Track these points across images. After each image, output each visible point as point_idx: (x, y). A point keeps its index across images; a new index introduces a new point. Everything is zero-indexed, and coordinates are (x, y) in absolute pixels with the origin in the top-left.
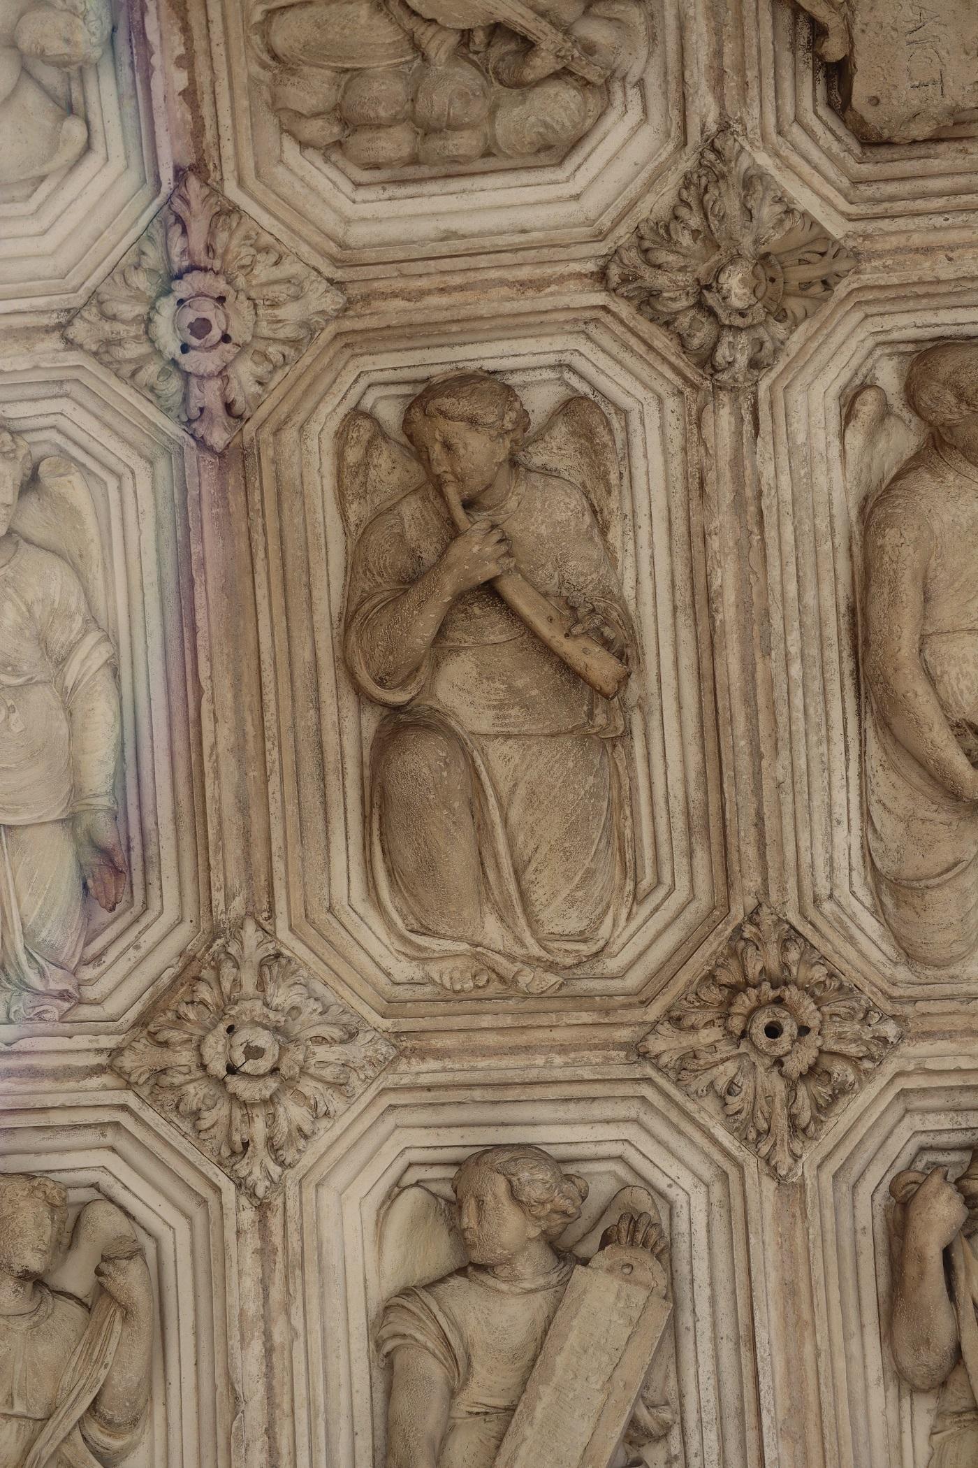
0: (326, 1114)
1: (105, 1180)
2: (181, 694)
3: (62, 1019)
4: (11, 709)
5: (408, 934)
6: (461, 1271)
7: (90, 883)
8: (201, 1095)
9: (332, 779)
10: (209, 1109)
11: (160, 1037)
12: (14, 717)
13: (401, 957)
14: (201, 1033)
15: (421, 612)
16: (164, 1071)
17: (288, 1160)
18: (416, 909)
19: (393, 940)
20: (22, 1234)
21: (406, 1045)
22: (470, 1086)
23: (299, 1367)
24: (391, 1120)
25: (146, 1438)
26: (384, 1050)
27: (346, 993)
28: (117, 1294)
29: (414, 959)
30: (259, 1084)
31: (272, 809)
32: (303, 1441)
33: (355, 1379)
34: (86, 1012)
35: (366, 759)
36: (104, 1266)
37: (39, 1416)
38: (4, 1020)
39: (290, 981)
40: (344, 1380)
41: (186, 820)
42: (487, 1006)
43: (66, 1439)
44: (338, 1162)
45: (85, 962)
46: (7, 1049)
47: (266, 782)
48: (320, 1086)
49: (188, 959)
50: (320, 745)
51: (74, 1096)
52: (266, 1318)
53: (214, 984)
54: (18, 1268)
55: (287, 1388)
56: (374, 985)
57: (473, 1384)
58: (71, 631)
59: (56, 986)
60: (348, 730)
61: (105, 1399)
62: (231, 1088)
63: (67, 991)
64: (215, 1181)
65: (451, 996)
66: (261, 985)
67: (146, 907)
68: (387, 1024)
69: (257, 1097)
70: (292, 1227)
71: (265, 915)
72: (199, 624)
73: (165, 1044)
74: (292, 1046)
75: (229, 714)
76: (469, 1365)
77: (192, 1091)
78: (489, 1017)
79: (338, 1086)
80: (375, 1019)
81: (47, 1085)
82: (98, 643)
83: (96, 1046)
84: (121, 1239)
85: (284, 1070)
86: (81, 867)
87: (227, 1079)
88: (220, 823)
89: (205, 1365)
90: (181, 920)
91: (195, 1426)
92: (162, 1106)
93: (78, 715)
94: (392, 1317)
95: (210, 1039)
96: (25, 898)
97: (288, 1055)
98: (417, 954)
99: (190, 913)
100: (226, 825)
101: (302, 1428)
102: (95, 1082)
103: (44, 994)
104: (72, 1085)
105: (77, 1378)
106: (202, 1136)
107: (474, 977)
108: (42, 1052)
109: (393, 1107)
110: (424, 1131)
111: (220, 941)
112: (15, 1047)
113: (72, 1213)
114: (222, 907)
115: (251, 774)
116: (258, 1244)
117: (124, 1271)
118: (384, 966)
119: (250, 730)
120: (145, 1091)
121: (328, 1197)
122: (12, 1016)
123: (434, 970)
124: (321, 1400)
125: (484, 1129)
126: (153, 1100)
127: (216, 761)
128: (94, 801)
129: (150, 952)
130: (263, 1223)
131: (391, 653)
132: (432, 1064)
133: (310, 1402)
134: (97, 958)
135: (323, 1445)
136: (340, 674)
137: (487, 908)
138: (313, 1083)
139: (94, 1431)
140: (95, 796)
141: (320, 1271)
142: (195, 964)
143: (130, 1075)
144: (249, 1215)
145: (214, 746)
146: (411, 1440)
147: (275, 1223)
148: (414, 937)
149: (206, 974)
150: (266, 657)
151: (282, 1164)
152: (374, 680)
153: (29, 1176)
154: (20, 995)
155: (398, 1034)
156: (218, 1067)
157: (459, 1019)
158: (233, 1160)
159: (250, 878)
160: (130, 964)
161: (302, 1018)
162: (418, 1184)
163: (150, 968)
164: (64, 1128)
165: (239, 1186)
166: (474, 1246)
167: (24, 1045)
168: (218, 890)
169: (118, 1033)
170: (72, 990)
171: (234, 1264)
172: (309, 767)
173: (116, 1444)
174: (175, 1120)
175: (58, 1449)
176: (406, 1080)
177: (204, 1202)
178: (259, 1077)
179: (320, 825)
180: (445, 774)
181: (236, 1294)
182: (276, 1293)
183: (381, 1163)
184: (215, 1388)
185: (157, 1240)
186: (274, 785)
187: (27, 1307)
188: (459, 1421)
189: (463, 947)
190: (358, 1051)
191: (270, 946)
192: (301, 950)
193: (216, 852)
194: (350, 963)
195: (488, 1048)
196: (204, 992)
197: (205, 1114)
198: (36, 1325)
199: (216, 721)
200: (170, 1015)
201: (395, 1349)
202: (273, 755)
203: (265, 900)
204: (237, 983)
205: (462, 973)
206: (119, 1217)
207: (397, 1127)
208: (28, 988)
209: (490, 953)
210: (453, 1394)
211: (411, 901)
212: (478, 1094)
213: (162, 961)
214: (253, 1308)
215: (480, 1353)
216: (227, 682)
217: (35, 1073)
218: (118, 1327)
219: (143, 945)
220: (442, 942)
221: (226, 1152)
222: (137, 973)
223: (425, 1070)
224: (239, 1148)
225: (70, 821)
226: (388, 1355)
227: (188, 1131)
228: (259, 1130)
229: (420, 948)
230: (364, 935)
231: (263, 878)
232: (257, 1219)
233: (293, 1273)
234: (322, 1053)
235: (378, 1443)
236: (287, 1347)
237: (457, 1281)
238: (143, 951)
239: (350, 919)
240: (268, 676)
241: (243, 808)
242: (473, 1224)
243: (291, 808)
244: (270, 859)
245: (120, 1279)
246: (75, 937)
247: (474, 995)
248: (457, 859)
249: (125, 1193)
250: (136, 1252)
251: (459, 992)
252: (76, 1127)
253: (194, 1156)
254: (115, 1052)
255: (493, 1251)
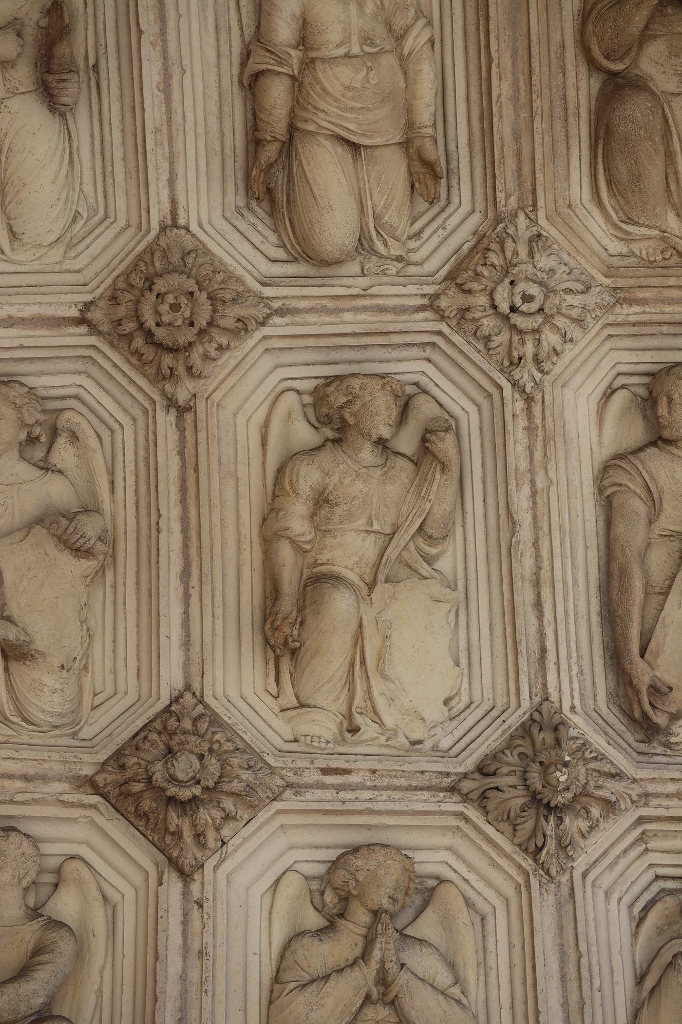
0: (571, 340)
1: (423, 381)
2: (476, 61)
3: (398, 274)
4: (370, 69)
5: (619, 223)
6: (653, 444)
7: (417, 185)
8: (491, 325)
9: (571, 119)
10: (497, 335)
11: (466, 287)
12: (372, 74)
13: (614, 239)
14: (492, 285)
15: (638, 11)
16: (468, 310)
17: (546, 369)
18: (625, 207)
19: (609, 227)
20: (377, 414)
21: (622, 296)
22: (660, 324)
23: (554, 504)
24: (608, 345)
25: (450, 548)
26: (607, 299)
27: (583, 261)
28: (436, 451)
29: (623, 240)
30: (530, 319)
31: (536, 139)
32: (557, 551)
33: (587, 514)
34: (412, 270)
35: (593, 107)
36: (429, 436)
37: (388, 532)
38: (360, 274)
39: (548, 252)
40: (580, 513)
41: (478, 145)
42: (671, 271)
43: (405, 547)
44: (576, 371)
45: (410, 238)
46: (364, 293)
47: (532, 121)
48: (567, 321)
49: (480, 237)
50: (565, 98)
51: (408, 325)
52: (532, 472)
53: (499, 253)
54: (375, 436)
55: (546, 517)
56: (598, 256)
57: (662, 517)
58: (408, 18)
59: (395, 252)
60: (582, 88)
61: (429, 522)
62: (512, 321)
63: (401, 256)
64: (499, 382)
65: (648, 264)
66: (531, 254)
67: (449, 202)
68: (608, 281)
69: (530, 327)
70: (548, 413)
71: (530, 208)
72: (491, 15)
73: (469, 292)
74: (552, 295)
75: (509, 75)
76: (661, 504)
77: (486, 323)
78: (674, 279)
79: (579, 322)
80: (601, 279)
81: (389, 317)
82: (425, 26)
83: (422, 292)
84: (438, 419)
85: (547, 310)
86: (410, 174)
87: (510, 315)
88: (502, 147)
89: (491, 501)
90: (473, 211)
91: (484, 540)
92: (465, 332)
93: (411, 73)
94: (611, 472)
95: (500, 289)
96: (375, 194)
97: (550, 300)
98: (625, 237)
99: (479, 206)
100: (506, 148)
101: (556, 543)
102: (420, 316)
103: (386, 258)
104: (405, 317)
105: (411, 508)
106: (491, 352)
107: (662, 252)
108: (387, 296)
109: (610, 336)
110: (628, 353)
111: (501, 225)
112: (369, 292)
113: (406, 398)
114: (503, 202)
115: (522, 115)
116: (526, 424)
117: (443, 439)
118: (603, 244)
119: (522, 86)
120: (454, 323)
121: (568, 394)
122: (365, 272)
123: (635, 247)
124: (567, 525)
125: (666, 352)
126: (459, 328)
127: (501, 106)
128: (422, 131)
129: (453, 231)
130: (529, 410)
131: (616, 37)
132: (637, 309)
133: (561, 526)
134: (417, 235)
135: (569, 555)
136: (578, 50)
137: (669, 207)
138: (563, 320)
139: (420, 542)
140: (424, 127)
141: (565, 442)
142: (485, 240)
143: (444, 312)
144: (520, 405)
145: (499, 96)
146: (627, 552)
147: (537, 410)
148: (623, 226)
149: (493, 246)
150: (534, 38)
151: (542, 372)
152: (603, 55)
153: (381, 376)
154: (370, 258)
155: (615, 289)
156: (504, 308)
157: (654, 279)
158: (510, 368)
159: (521, 184)
160: (439, 239)
161: (557, 276)
162: (623, 387)
163: (453, 243)
164: (399, 345)
165: (514, 386)
166: (665, 427)
167: (375, 290)
168: (501, 191)
169: (434, 284)
170: (404, 255)
171: (511, 436)
172: (558, 112)
173: (433, 551)
174: (473, 341)
175: (400, 554)
176: (620, 319)
177: (490, 396)
178: (531, 314)
179: (564, 151)
180: (651, 118)
181: (513, 456)
182: (538, 455)
183: (600, 374)
184: (498, 516)
185: (456, 420)
186: (537, 123)
187: (379, 461)
188: (652, 541)
189: (655, 232)
190: (591, 299)
191: (534, 229)
192: (554, 232)
193: (500, 166)
194: (583, 241)
195: (672, 299)
196: (494, 258)
197: (494, 338)
198: (385, 473)
199: (501, 79)
200: (470, 272)
201: (614, 493)
202: (537, 103)
203: (530, 199)
204: (516, 253)
205: (654, 249)
206: (434, 405)
207: (611, 349)
208: (376, 253)
209: (672, 237)
210: (650, 522)
211: (622, 202)
212: (665, 329)
213: (463, 237)
214: (523, 465)
215: (668, 497)
216: (508, 54)
217: (382, 309)
218: (438, 475)
219: (448, 227)
220: (641, 229)
221: (506, 363)
222: (445, 245)
223: (633, 313)
224: (516, 360)
225: (406, 144)
226: (608, 496)
227: (481, 349)
228: (529, 349)
229: (627, 233)
230: (591, 224)
231: (529, 184)
232: (525, 407)
233: (549, 442)
234: (570, 299)
235: (601, 554)
236: (545, 490)
237: (652, 451)
238: (448, 231)
239: (582, 213)
240: (535, 51)
241: (517, 138)
242: (665, 413)
243: (547, 138)
244: (534, 172)
245: (440, 444)
246: (405, 220)
247: (662, 264)
248: (655, 174)
249: (436, 389)
250: (447, 429)
251: (652, 262)
252: (407, 345)
253: (485, 366)
254: (435, 297)
255: (678, 431)
